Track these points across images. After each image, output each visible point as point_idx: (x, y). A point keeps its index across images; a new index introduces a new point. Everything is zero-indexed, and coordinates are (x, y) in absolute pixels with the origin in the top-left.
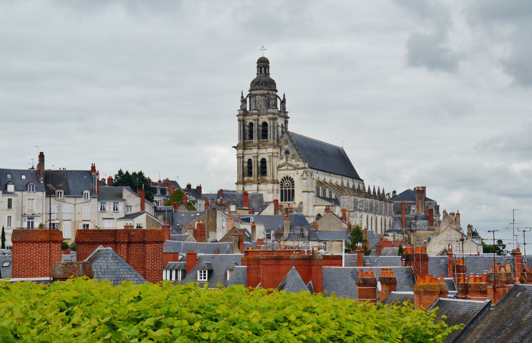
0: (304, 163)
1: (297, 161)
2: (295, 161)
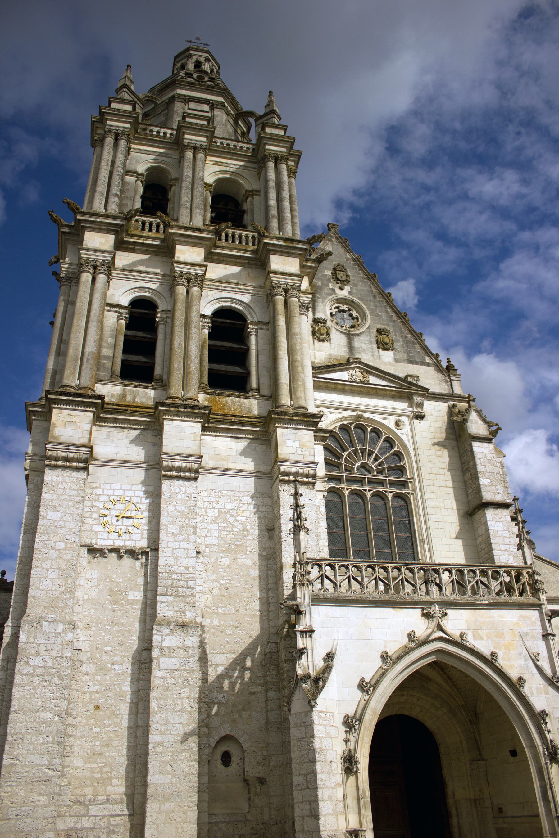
0: (440, 376)
1: (411, 362)
2: (396, 360)
